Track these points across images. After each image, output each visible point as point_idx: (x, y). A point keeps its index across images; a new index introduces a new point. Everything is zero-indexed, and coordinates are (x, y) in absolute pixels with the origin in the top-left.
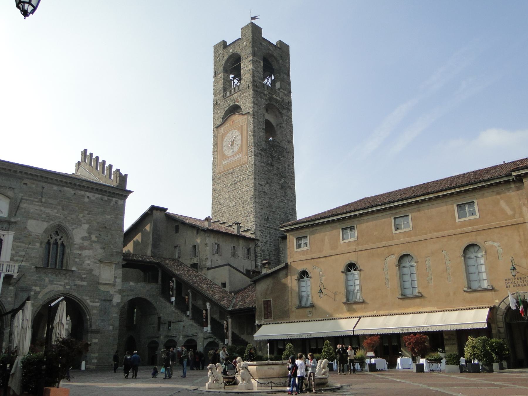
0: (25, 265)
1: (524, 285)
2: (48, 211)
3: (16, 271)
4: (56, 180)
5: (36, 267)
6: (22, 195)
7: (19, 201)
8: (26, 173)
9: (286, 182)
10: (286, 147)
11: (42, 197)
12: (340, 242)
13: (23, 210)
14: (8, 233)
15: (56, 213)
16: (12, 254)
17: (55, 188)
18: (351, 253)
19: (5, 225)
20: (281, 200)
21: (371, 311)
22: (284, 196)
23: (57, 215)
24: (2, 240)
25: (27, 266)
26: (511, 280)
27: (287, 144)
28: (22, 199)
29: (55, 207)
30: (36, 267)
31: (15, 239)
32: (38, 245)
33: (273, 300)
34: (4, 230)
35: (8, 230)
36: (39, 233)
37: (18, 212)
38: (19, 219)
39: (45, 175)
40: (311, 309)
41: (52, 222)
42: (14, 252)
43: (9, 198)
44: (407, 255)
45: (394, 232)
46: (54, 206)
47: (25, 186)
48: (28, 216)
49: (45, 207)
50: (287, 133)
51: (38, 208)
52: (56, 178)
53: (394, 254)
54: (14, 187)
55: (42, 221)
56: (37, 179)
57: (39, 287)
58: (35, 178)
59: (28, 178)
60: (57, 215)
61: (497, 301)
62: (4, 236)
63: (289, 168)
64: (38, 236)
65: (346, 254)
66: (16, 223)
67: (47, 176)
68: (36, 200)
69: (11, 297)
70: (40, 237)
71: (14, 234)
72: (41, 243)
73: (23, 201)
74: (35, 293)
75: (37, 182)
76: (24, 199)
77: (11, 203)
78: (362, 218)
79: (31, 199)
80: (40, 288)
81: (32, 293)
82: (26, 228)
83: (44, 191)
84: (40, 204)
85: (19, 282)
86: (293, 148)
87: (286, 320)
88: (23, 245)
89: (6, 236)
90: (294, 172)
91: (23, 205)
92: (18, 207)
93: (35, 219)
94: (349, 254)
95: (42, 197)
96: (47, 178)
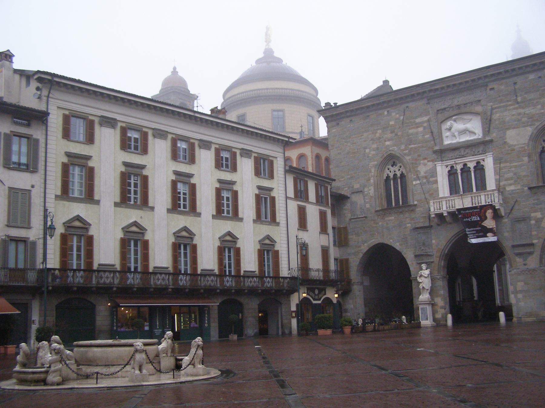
0: (516, 188)
2: (529, 110)
3: (496, 200)
4: (527, 67)
5: (530, 188)
6: (491, 104)
7: (489, 113)
8: (486, 77)
11: (516, 96)
13: (497, 122)
14: (486, 156)
15: (541, 110)
16: (496, 180)
17: (531, 76)
19: (481, 149)
23: (542, 111)
24: (483, 166)
25: (518, 189)
28: (492, 109)
29: (537, 102)
30: (530, 188)
31: (497, 161)
32: (526, 159)
34: (481, 154)
35: (484, 152)
36: (524, 144)
37: (491, 128)
38: (494, 135)
39: (509, 68)
41: (537, 124)
42: (498, 177)
43: (479, 114)
46: (535, 102)
47: (492, 91)
48: (505, 127)
49: (523, 108)
51: (514, 113)
52: (525, 65)
54: (480, 99)
55: (524, 126)
56: (502, 77)
57: (539, 213)
58: (500, 76)
59: (493, 81)
60: (542, 111)
62: (484, 161)
64: (522, 147)
66: (491, 141)
67: (512, 68)
68: (510, 103)
69: (508, 232)
70: (526, 148)
71: (493, 154)
72: (529, 156)
73: (494, 111)
74: (536, 222)
75: (505, 81)
76: (496, 108)
77: (482, 120)
79: (502, 104)
80: (541, 214)
81: (533, 222)
82: (505, 142)
83: (516, 87)
84: (517, 106)
85: (512, 211)
88: (508, 164)
89: (485, 160)
91: (496, 116)
92: (490, 120)
93: (514, 128)
95: (516, 96)
96: (513, 70)
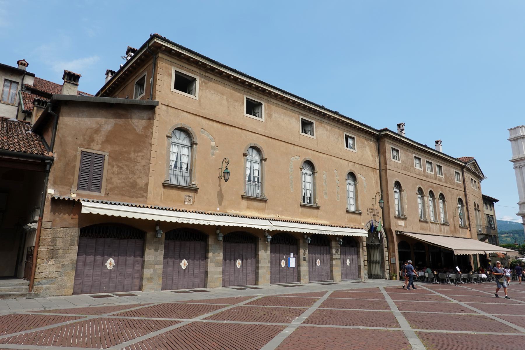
18: (257, 135)
21: (274, 214)
33: (109, 156)
40: (192, 194)
53: (299, 156)
87: (139, 202)
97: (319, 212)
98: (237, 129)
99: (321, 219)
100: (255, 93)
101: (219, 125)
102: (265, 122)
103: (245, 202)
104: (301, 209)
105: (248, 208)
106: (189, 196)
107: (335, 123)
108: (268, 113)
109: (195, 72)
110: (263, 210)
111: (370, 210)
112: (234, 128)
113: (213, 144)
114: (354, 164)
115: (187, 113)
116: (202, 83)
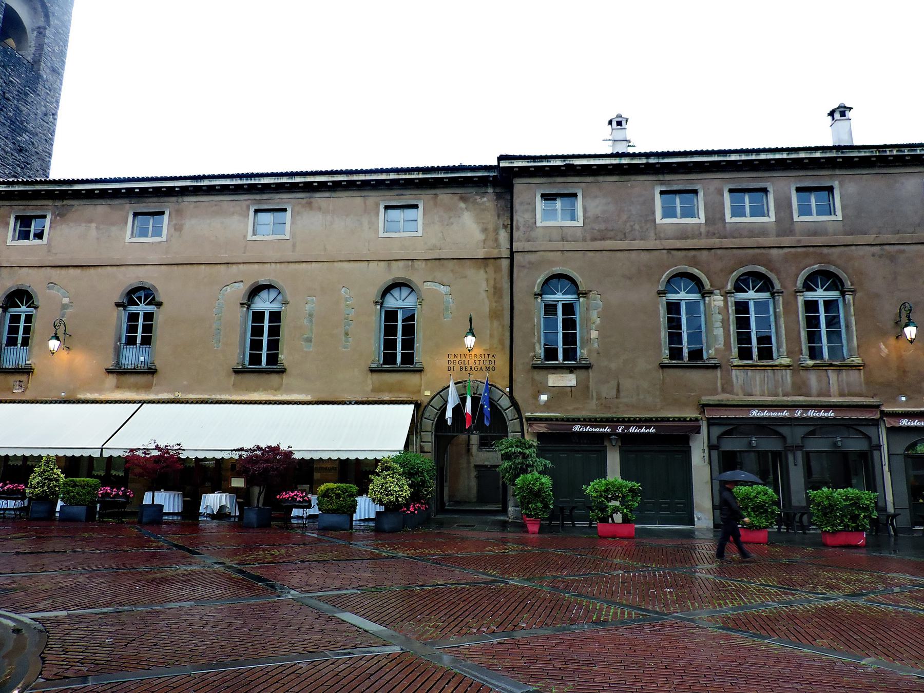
1: (479, 368)
9: (33, 144)
10: (45, 76)
12: (124, 239)
20: (13, 173)
22: (22, 168)
26: (459, 357)
27: (48, 71)
40: (24, 378)
44: (269, 287)
45: (249, 237)
50: (54, 51)
53: (242, 281)
61: (428, 393)
63: (46, 118)
65: (134, 267)
78: (186, 199)
86: (61, 84)
90: (54, 131)
94: (140, 268)
97: (286, 379)
98: (109, 268)
99: (290, 390)
100: (151, 200)
101: (78, 271)
102: (167, 241)
103: (112, 380)
104: (233, 377)
105: (118, 387)
106: (20, 381)
107: (352, 192)
108: (176, 224)
109: (45, 207)
110: (148, 387)
111: (457, 360)
112: (104, 268)
113: (66, 301)
114: (410, 262)
115: (27, 269)
116: (56, 218)
